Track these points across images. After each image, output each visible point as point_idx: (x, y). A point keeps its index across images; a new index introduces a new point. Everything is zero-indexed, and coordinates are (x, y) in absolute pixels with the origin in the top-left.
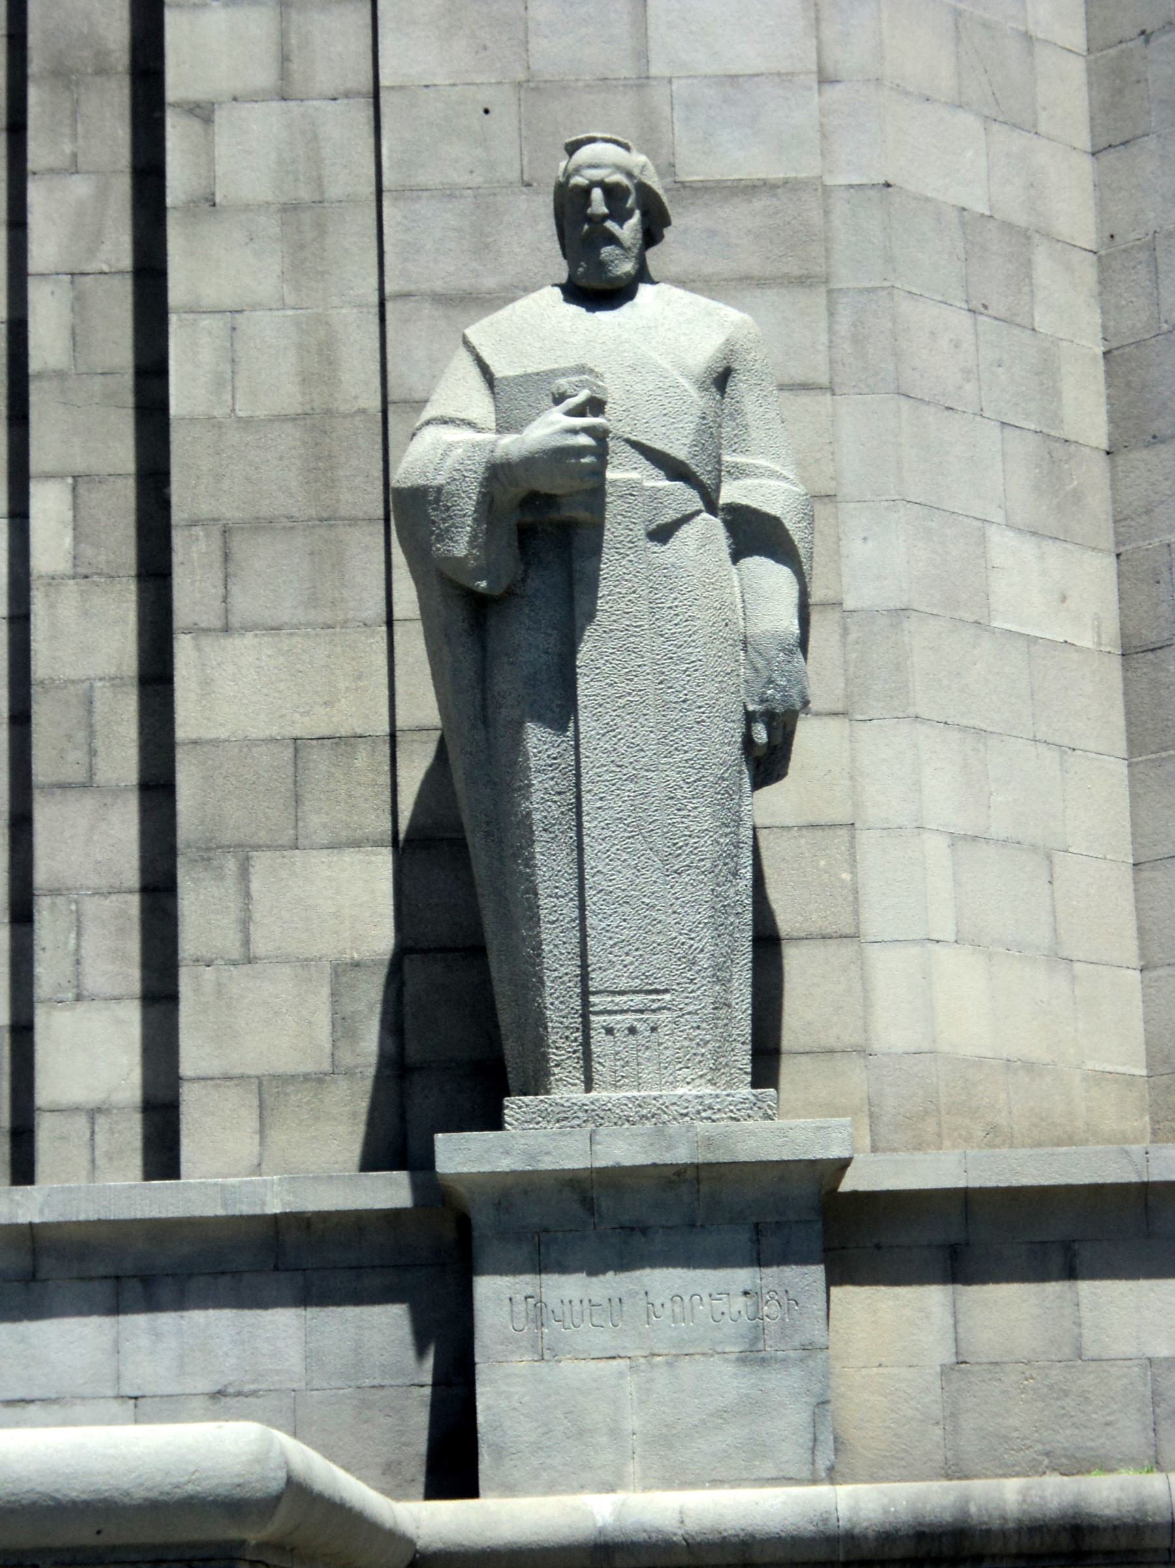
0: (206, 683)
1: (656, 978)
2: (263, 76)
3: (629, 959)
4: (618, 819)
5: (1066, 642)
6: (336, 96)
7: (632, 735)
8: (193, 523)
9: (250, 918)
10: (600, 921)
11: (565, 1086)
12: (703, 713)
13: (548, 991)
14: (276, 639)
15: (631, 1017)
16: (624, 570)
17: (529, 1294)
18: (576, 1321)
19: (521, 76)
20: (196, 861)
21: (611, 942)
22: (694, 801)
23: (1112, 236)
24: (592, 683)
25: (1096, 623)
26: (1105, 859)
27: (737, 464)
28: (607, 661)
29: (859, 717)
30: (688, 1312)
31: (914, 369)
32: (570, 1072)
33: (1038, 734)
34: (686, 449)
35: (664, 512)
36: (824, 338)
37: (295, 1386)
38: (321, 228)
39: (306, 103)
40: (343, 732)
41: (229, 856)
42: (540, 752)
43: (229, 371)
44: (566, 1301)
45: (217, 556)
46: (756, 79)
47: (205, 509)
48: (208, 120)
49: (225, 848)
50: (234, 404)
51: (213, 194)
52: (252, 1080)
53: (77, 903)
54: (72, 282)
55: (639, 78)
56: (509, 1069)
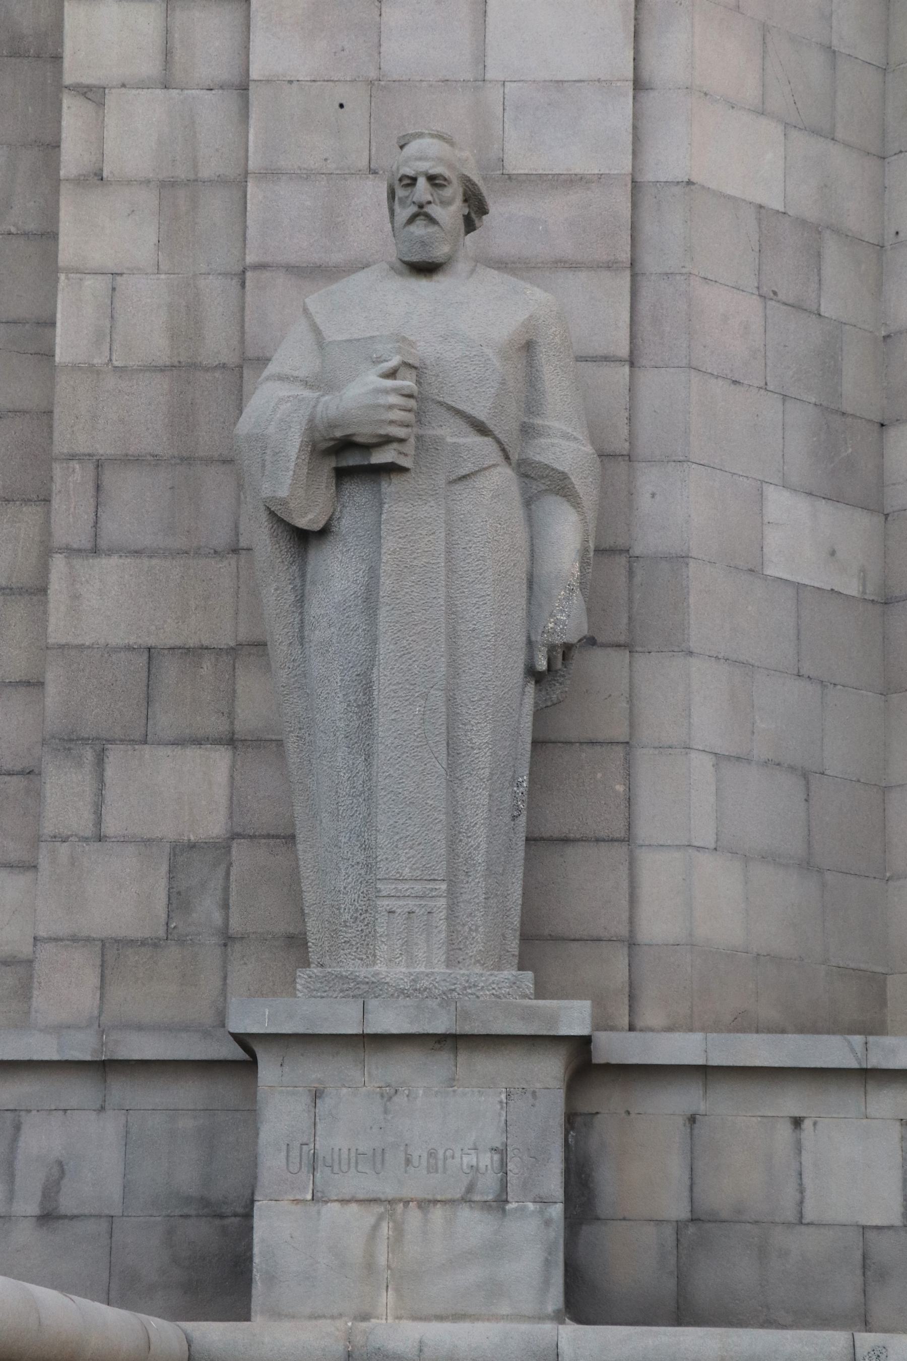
3: (412, 852)
4: (409, 730)
5: (832, 590)
6: (212, 88)
7: (425, 658)
8: (72, 457)
9: (103, 802)
12: (489, 641)
14: (138, 561)
15: (411, 904)
17: (305, 1141)
18: (345, 1168)
19: (373, 74)
23: (897, 233)
25: (862, 574)
26: (859, 781)
28: (407, 593)
29: (639, 649)
30: (440, 1164)
33: (801, 670)
39: (186, 92)
40: (191, 643)
41: (88, 747)
44: (336, 1149)
45: (90, 487)
46: (578, 84)
47: (82, 445)
48: (101, 105)
49: (85, 740)
50: (111, 354)
51: (102, 170)
52: (97, 943)
56: (310, 944)
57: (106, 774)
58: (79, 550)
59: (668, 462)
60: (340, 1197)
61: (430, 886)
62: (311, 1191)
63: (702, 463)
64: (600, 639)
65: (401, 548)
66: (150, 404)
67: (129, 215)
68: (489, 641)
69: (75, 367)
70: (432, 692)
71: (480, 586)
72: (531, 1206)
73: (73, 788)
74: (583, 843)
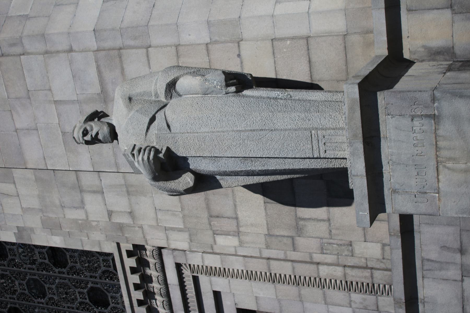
0: (252, 225)
1: (307, 136)
2: (99, 197)
3: (301, 144)
4: (257, 146)
9: (317, 219)
10: (290, 153)
11: (347, 163)
12: (223, 115)
13: (316, 167)
14: (238, 205)
15: (320, 145)
16: (181, 141)
17: (414, 196)
20: (301, 232)
21: (296, 150)
22: (251, 118)
24: (216, 152)
27: (154, 95)
29: (241, 37)
31: (142, 20)
32: (342, 162)
34: (146, 118)
35: (164, 127)
36: (134, 51)
37: (459, 230)
38: (132, 186)
39: (103, 187)
41: (299, 223)
42: (240, 167)
43: (170, 212)
44: (416, 184)
45: (217, 219)
48: (112, 212)
49: (297, 224)
50: (178, 211)
51: (129, 212)
53: (324, 244)
54: (168, 230)
55: (78, 103)
57: (307, 218)
58: (237, 223)
59: (178, 31)
60: (437, 183)
61: (313, 136)
62: (435, 194)
63: (177, 18)
64: (238, 53)
65: (194, 150)
66: (190, 200)
67: (139, 205)
68: (223, 115)
69: (184, 222)
70: (242, 137)
71: (204, 119)
72: (436, 104)
73: (313, 228)
74: (310, 55)
